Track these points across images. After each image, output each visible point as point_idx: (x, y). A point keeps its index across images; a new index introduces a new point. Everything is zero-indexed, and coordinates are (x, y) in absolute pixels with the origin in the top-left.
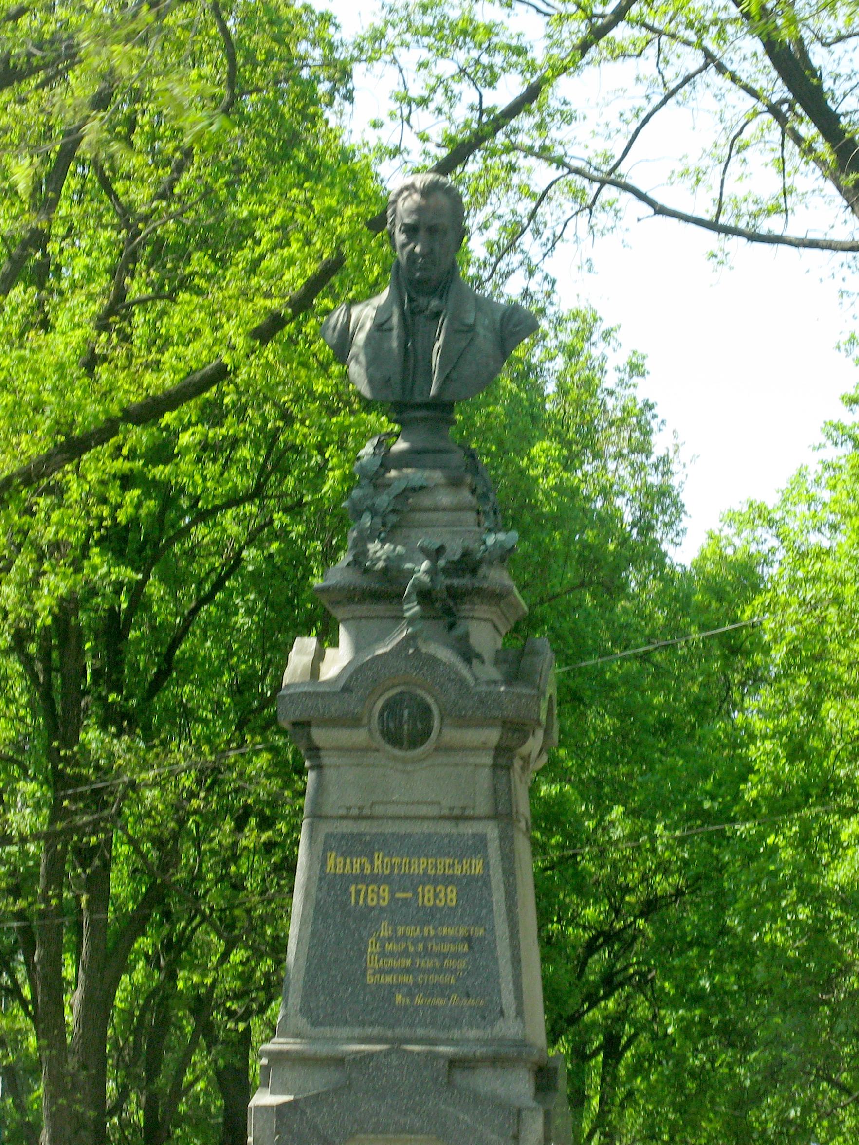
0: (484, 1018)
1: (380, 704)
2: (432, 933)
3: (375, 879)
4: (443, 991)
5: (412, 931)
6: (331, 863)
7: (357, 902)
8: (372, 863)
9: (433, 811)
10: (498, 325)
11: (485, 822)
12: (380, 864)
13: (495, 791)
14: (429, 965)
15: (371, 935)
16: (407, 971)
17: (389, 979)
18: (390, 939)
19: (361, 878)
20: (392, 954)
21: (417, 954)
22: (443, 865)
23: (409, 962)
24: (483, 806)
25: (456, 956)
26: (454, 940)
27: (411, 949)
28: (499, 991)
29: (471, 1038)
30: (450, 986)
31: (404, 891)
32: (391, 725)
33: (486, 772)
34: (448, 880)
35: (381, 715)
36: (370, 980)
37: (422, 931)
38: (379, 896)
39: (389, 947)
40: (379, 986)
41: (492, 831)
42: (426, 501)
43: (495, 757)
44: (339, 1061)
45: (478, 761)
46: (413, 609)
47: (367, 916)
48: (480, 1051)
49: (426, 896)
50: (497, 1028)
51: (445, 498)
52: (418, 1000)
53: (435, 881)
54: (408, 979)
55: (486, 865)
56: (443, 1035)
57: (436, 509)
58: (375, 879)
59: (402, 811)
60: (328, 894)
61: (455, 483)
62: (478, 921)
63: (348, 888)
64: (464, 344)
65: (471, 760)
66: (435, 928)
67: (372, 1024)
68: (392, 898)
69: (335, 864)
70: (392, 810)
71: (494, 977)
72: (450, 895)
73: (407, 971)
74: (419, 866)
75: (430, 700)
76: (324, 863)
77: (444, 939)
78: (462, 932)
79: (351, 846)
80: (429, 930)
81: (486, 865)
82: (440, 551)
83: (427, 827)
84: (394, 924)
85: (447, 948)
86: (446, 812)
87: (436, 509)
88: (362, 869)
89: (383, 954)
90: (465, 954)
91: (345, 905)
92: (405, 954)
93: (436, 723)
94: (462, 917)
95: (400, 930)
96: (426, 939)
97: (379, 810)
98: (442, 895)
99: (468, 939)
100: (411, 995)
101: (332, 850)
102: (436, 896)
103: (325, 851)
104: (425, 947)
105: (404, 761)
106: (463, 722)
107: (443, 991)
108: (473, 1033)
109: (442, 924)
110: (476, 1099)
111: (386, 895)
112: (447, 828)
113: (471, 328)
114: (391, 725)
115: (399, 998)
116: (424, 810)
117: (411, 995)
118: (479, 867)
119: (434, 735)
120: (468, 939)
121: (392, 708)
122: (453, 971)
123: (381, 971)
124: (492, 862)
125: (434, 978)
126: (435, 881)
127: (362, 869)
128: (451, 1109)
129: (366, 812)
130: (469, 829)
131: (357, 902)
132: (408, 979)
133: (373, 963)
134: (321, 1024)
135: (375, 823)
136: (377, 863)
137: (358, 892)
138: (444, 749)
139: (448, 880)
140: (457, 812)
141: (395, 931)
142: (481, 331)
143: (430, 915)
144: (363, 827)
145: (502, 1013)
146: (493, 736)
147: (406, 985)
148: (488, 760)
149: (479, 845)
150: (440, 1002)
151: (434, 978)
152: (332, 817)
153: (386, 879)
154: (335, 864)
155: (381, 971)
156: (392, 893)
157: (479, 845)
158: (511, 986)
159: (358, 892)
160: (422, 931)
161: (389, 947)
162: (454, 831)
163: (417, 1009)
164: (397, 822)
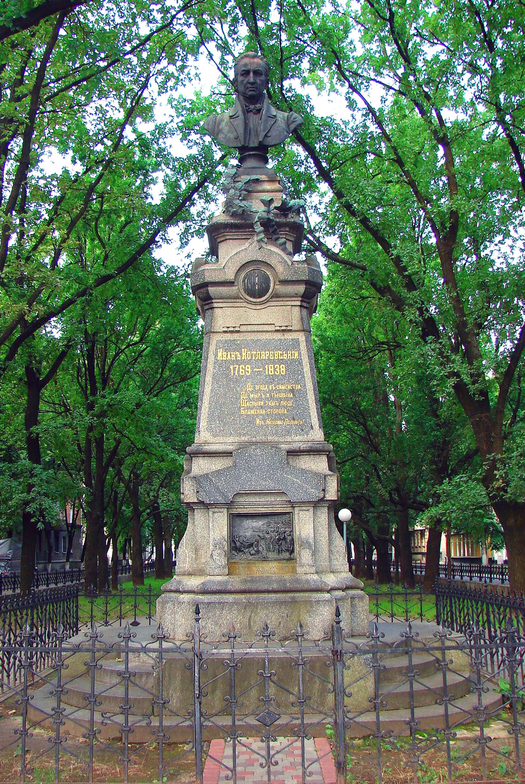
1: (243, 275)
2: (274, 388)
3: (243, 362)
4: (281, 417)
5: (263, 388)
6: (220, 354)
7: (234, 374)
8: (241, 354)
9: (272, 328)
10: (286, 118)
11: (298, 333)
12: (245, 354)
14: (273, 404)
15: (242, 390)
18: (252, 392)
19: (237, 362)
23: (262, 403)
24: (296, 325)
25: (287, 399)
26: (285, 391)
27: (263, 396)
31: (258, 368)
32: (249, 285)
33: (298, 308)
34: (281, 362)
35: (244, 281)
36: (243, 412)
37: (268, 387)
38: (246, 370)
39: (252, 396)
40: (248, 416)
41: (301, 337)
42: (260, 188)
43: (301, 301)
44: (228, 454)
45: (293, 303)
46: (259, 228)
48: (303, 446)
49: (270, 370)
50: (310, 435)
51: (268, 186)
55: (300, 354)
57: (264, 191)
58: (243, 362)
59: (255, 328)
62: (297, 382)
65: (289, 303)
66: (275, 386)
67: (244, 435)
70: (249, 328)
71: (307, 409)
76: (216, 355)
77: (280, 391)
78: (289, 387)
79: (229, 346)
81: (300, 354)
82: (271, 201)
83: (267, 336)
84: (253, 384)
85: (282, 395)
86: (278, 328)
87: (264, 191)
88: (236, 357)
90: (292, 398)
91: (227, 375)
92: (260, 399)
93: (272, 285)
94: (288, 380)
96: (270, 392)
97: (243, 328)
98: (278, 370)
99: (292, 391)
100: (264, 420)
101: (220, 348)
102: (275, 370)
103: (216, 349)
106: (284, 282)
108: (297, 438)
109: (278, 384)
111: (249, 370)
112: (278, 336)
113: (275, 116)
114: (249, 285)
115: (258, 421)
116: (266, 328)
118: (296, 355)
119: (270, 291)
120: (292, 391)
122: (285, 407)
123: (249, 408)
125: (276, 411)
126: (274, 362)
127: (236, 357)
128: (289, 477)
129: (237, 329)
130: (289, 336)
131: (234, 374)
134: (218, 436)
135: (242, 334)
136: (244, 354)
137: (234, 369)
138: (276, 296)
139: (281, 362)
144: (236, 336)
145: (312, 428)
146: (301, 289)
148: (299, 303)
149: (295, 344)
150: (279, 422)
151: (276, 411)
152: (219, 332)
153: (249, 362)
155: (249, 408)
156: (252, 368)
158: (316, 414)
159: (234, 369)
160: (268, 387)
161: (252, 396)
162: (282, 338)
163: (267, 426)
164: (253, 334)
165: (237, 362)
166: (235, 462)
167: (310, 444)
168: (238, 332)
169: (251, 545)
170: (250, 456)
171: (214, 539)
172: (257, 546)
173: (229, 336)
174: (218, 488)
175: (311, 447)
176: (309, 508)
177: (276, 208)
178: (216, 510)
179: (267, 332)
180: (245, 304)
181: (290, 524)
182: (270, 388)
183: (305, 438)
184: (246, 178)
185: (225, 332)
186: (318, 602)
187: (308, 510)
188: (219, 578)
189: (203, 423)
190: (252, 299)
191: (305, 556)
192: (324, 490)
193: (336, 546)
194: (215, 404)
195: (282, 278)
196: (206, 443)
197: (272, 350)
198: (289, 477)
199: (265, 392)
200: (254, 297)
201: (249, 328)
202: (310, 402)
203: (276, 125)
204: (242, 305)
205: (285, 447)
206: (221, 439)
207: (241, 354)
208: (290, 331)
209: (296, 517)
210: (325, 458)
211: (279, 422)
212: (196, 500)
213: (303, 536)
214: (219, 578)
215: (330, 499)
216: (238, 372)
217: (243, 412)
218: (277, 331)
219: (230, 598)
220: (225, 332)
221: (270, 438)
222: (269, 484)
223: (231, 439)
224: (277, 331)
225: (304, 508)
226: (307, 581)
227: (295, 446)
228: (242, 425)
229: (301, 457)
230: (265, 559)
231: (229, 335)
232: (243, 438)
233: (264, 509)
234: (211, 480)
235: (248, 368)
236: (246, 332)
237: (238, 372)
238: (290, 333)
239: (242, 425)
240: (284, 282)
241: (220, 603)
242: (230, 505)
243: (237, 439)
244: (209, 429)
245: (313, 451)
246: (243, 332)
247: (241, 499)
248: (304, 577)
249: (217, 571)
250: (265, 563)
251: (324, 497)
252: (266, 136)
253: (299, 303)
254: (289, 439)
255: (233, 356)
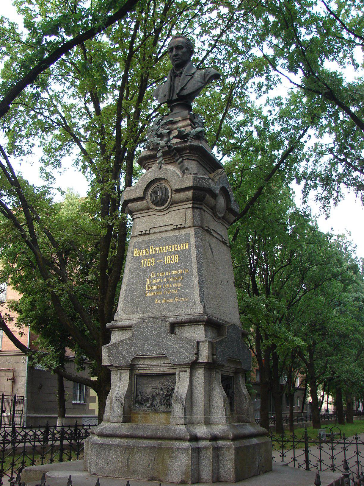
0: (187, 305)
4: (172, 296)
6: (135, 252)
7: (143, 266)
8: (149, 251)
12: (152, 250)
13: (193, 217)
15: (147, 278)
16: (160, 290)
17: (153, 294)
18: (154, 279)
19: (146, 257)
20: (155, 284)
21: (164, 283)
22: (175, 248)
23: (161, 286)
24: (189, 223)
25: (178, 282)
26: (177, 276)
27: (162, 281)
28: (194, 294)
29: (183, 314)
30: (175, 294)
33: (190, 211)
34: (175, 253)
36: (147, 295)
37: (166, 274)
38: (150, 263)
39: (154, 281)
40: (149, 297)
41: (192, 231)
43: (193, 203)
47: (146, 271)
48: (185, 318)
49: (167, 260)
52: (164, 301)
53: (171, 254)
54: (160, 293)
55: (189, 246)
56: (172, 314)
58: (150, 256)
60: (134, 264)
61: (184, 119)
62: (186, 267)
63: (140, 261)
64: (189, 79)
67: (146, 312)
68: (156, 262)
69: (136, 253)
70: (156, 230)
72: (176, 258)
73: (160, 290)
74: (166, 249)
75: (168, 186)
77: (173, 276)
80: (168, 273)
84: (156, 272)
85: (174, 279)
86: (175, 227)
89: (152, 284)
90: (181, 280)
91: (140, 267)
92: (159, 283)
93: (170, 195)
95: (158, 274)
96: (166, 277)
97: (152, 231)
100: (161, 299)
102: (171, 259)
103: (134, 249)
104: (167, 280)
105: (160, 211)
107: (172, 296)
110: (181, 339)
112: (176, 233)
115: (156, 300)
117: (161, 299)
119: (169, 199)
120: (182, 275)
121: (154, 192)
123: (151, 291)
124: (192, 243)
125: (169, 292)
126: (171, 254)
128: (171, 343)
129: (148, 232)
130: (183, 232)
131: (143, 266)
132: (160, 293)
133: (148, 288)
135: (151, 235)
138: (174, 203)
139: (175, 253)
140: (179, 226)
141: (156, 275)
142: (196, 75)
143: (170, 267)
144: (147, 237)
147: (159, 295)
150: (171, 301)
151: (169, 292)
153: (154, 256)
154: (136, 253)
155: (151, 291)
157: (187, 238)
158: (198, 291)
160: (166, 274)
161: (154, 281)
162: (178, 234)
163: (163, 304)
164: (159, 234)
165: (146, 257)
166: (133, 333)
167: (191, 316)
168: (149, 234)
169: (147, 400)
170: (144, 328)
171: (117, 394)
172: (152, 400)
173: (143, 238)
174: (122, 354)
175: (190, 319)
176: (187, 369)
177: (175, 137)
178: (122, 371)
179: (218, 234)
180: (154, 213)
181: (174, 383)
182: (167, 274)
183: (189, 312)
184: (165, 121)
185: (140, 235)
186: (178, 449)
187: (186, 371)
188: (115, 425)
189: (120, 306)
190: (157, 208)
191: (178, 410)
192: (197, 354)
193: (216, 402)
194: (131, 291)
195: (174, 188)
196: (121, 320)
197: (171, 245)
198: (171, 343)
199: (163, 278)
200: (159, 206)
201: (156, 230)
202: (195, 282)
203: (192, 80)
204: (152, 213)
205: (171, 320)
206: (131, 316)
207: (149, 251)
208: (184, 228)
209: (177, 376)
210: (202, 327)
211: (171, 301)
212: (109, 364)
213: (180, 392)
214: (115, 425)
215: (202, 361)
216: (147, 264)
217: (147, 295)
218: (175, 229)
219: (116, 441)
220: (140, 235)
221: (164, 313)
222: (157, 350)
223: (137, 316)
224: (175, 229)
225: (183, 369)
226: (175, 431)
227: (179, 319)
228: (146, 304)
229: (185, 327)
230: (156, 411)
231: (142, 237)
232: (145, 315)
233: (157, 370)
234: (118, 348)
235: (153, 260)
236: (154, 233)
237: (147, 264)
238: (184, 230)
239: (146, 304)
240: (178, 191)
241: (109, 445)
242: (132, 367)
243: (141, 316)
244: (124, 309)
245: (193, 322)
246: (152, 234)
247: (140, 363)
248: (174, 427)
249: (115, 419)
250: (156, 414)
251: (197, 359)
252: (182, 89)
253: (191, 205)
254: (177, 313)
255: (143, 253)
